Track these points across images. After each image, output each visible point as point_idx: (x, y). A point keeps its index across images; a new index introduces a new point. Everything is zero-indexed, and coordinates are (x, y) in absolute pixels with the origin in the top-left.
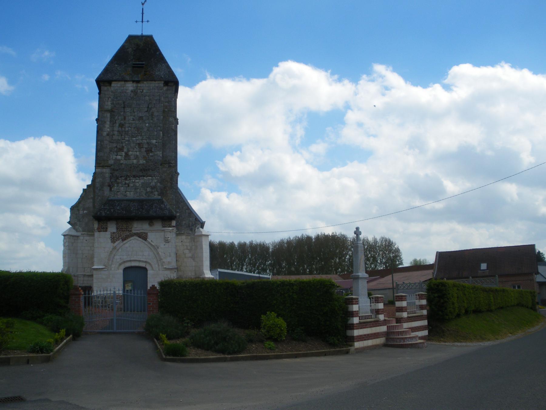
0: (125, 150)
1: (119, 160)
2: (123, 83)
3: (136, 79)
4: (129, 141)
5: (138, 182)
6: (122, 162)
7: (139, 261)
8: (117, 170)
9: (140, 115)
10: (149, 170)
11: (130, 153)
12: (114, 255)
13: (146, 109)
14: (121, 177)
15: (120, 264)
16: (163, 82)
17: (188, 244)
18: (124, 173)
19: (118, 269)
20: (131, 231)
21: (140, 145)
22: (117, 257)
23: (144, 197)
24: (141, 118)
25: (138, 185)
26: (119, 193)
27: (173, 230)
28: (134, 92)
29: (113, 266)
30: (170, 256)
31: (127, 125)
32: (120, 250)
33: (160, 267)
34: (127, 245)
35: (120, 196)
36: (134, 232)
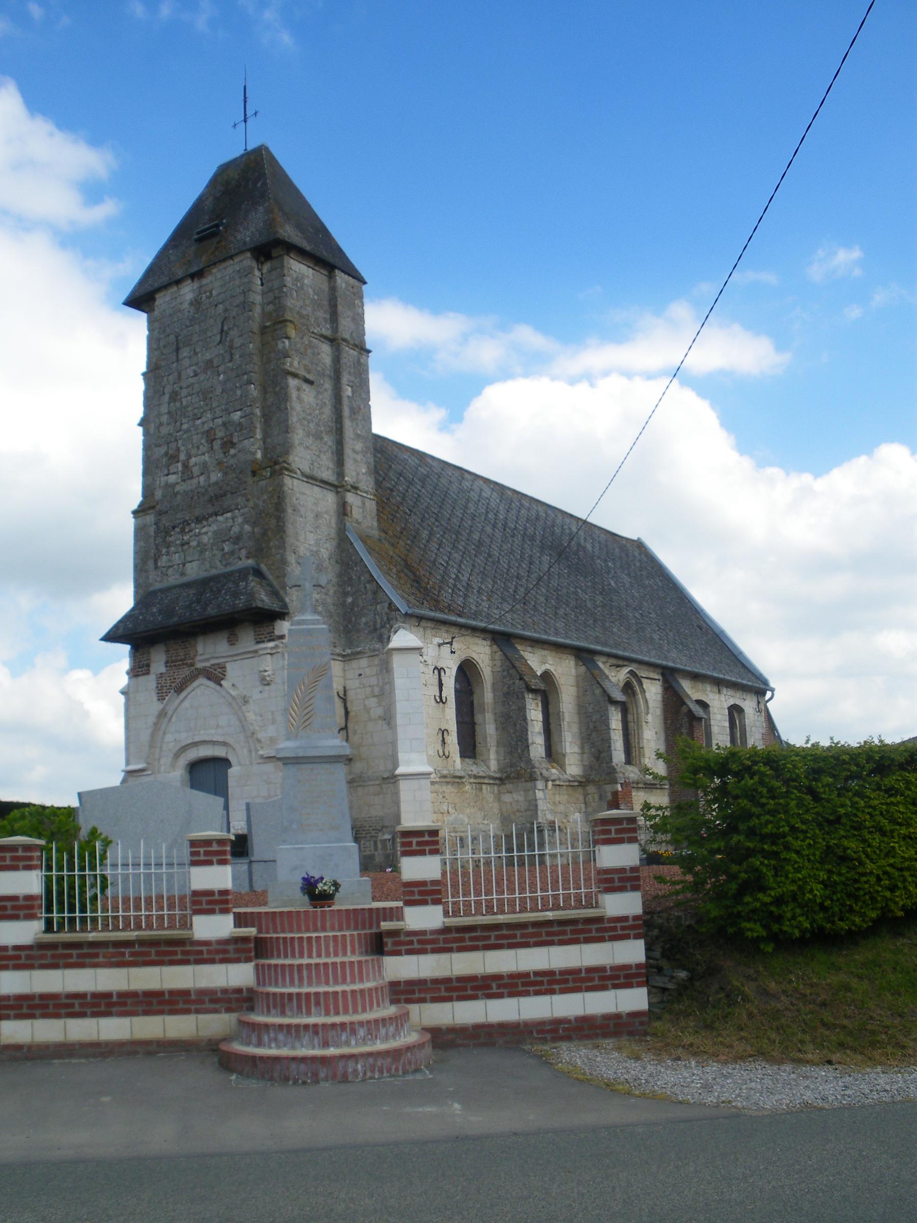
0: (182, 457)
1: (173, 486)
2: (175, 289)
3: (195, 269)
4: (188, 431)
5: (206, 533)
6: (178, 488)
7: (214, 743)
8: (166, 512)
9: (208, 356)
10: (225, 495)
11: (193, 460)
12: (165, 733)
13: (218, 338)
14: (174, 528)
15: (177, 755)
16: (249, 254)
17: (374, 681)
18: (179, 515)
19: (173, 766)
20: (192, 665)
21: (209, 435)
22: (169, 737)
23: (220, 569)
24: (209, 364)
25: (205, 539)
26: (170, 571)
27: (276, 647)
28: (196, 303)
29: (163, 761)
30: (274, 722)
31: (184, 392)
32: (174, 719)
33: (254, 754)
34: (186, 704)
35: (173, 579)
36: (199, 665)
